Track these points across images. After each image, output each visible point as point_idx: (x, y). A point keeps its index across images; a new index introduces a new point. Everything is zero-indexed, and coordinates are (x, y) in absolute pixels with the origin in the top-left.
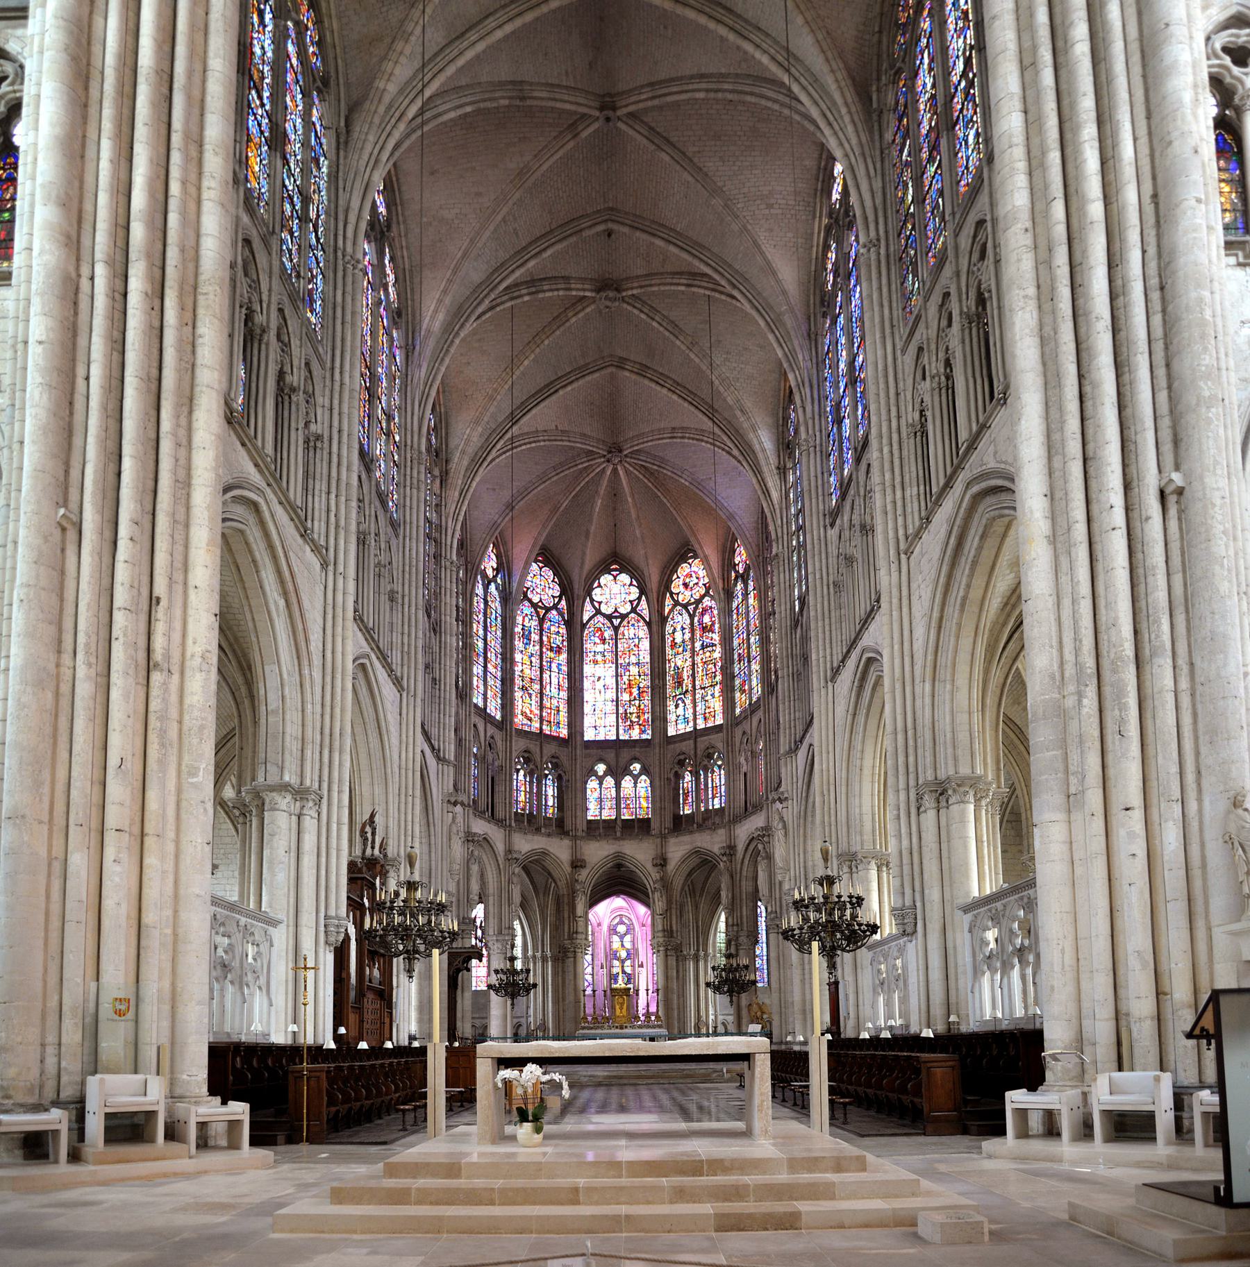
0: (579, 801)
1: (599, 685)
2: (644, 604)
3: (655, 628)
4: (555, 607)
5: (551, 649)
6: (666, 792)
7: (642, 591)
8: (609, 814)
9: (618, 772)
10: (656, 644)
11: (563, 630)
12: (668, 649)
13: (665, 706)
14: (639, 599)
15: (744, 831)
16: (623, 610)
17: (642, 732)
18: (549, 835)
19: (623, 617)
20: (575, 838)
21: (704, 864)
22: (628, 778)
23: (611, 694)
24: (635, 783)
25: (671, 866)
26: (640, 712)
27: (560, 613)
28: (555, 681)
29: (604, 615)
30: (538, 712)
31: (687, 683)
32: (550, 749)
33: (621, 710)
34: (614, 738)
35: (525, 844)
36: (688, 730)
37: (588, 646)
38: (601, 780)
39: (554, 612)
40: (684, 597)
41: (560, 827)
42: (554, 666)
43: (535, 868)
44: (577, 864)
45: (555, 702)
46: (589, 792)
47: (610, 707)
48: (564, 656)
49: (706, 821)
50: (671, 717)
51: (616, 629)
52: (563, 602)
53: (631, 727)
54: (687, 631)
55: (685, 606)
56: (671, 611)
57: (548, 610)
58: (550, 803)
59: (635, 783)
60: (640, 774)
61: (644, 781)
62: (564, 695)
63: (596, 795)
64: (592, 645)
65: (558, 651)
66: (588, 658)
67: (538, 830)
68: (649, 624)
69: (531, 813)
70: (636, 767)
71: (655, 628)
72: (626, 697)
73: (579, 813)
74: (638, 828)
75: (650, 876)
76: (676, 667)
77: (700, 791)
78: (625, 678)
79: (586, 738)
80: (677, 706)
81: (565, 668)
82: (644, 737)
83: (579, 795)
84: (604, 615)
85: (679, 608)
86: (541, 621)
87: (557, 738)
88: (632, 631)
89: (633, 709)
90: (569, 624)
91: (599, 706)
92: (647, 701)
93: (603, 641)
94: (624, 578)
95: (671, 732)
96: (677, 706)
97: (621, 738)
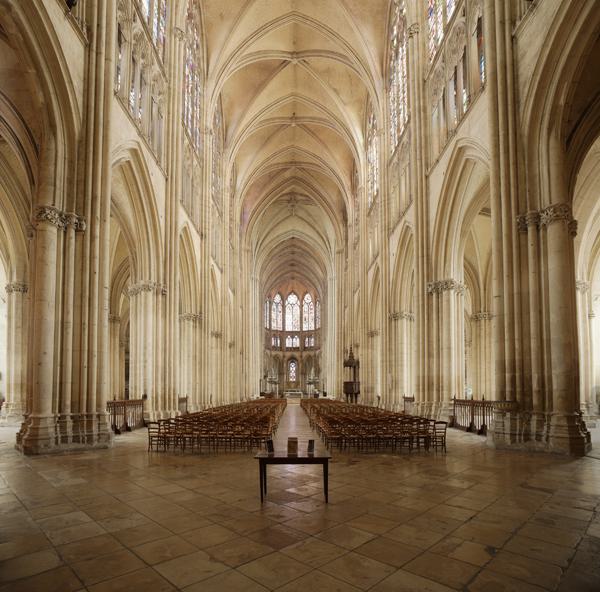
6: (302, 341)
9: (293, 337)
15: (317, 352)
21: (309, 358)
35: (274, 353)
41: (281, 349)
43: (276, 358)
44: (284, 356)
49: (310, 348)
64: (287, 310)
74: (296, 349)
75: (299, 359)
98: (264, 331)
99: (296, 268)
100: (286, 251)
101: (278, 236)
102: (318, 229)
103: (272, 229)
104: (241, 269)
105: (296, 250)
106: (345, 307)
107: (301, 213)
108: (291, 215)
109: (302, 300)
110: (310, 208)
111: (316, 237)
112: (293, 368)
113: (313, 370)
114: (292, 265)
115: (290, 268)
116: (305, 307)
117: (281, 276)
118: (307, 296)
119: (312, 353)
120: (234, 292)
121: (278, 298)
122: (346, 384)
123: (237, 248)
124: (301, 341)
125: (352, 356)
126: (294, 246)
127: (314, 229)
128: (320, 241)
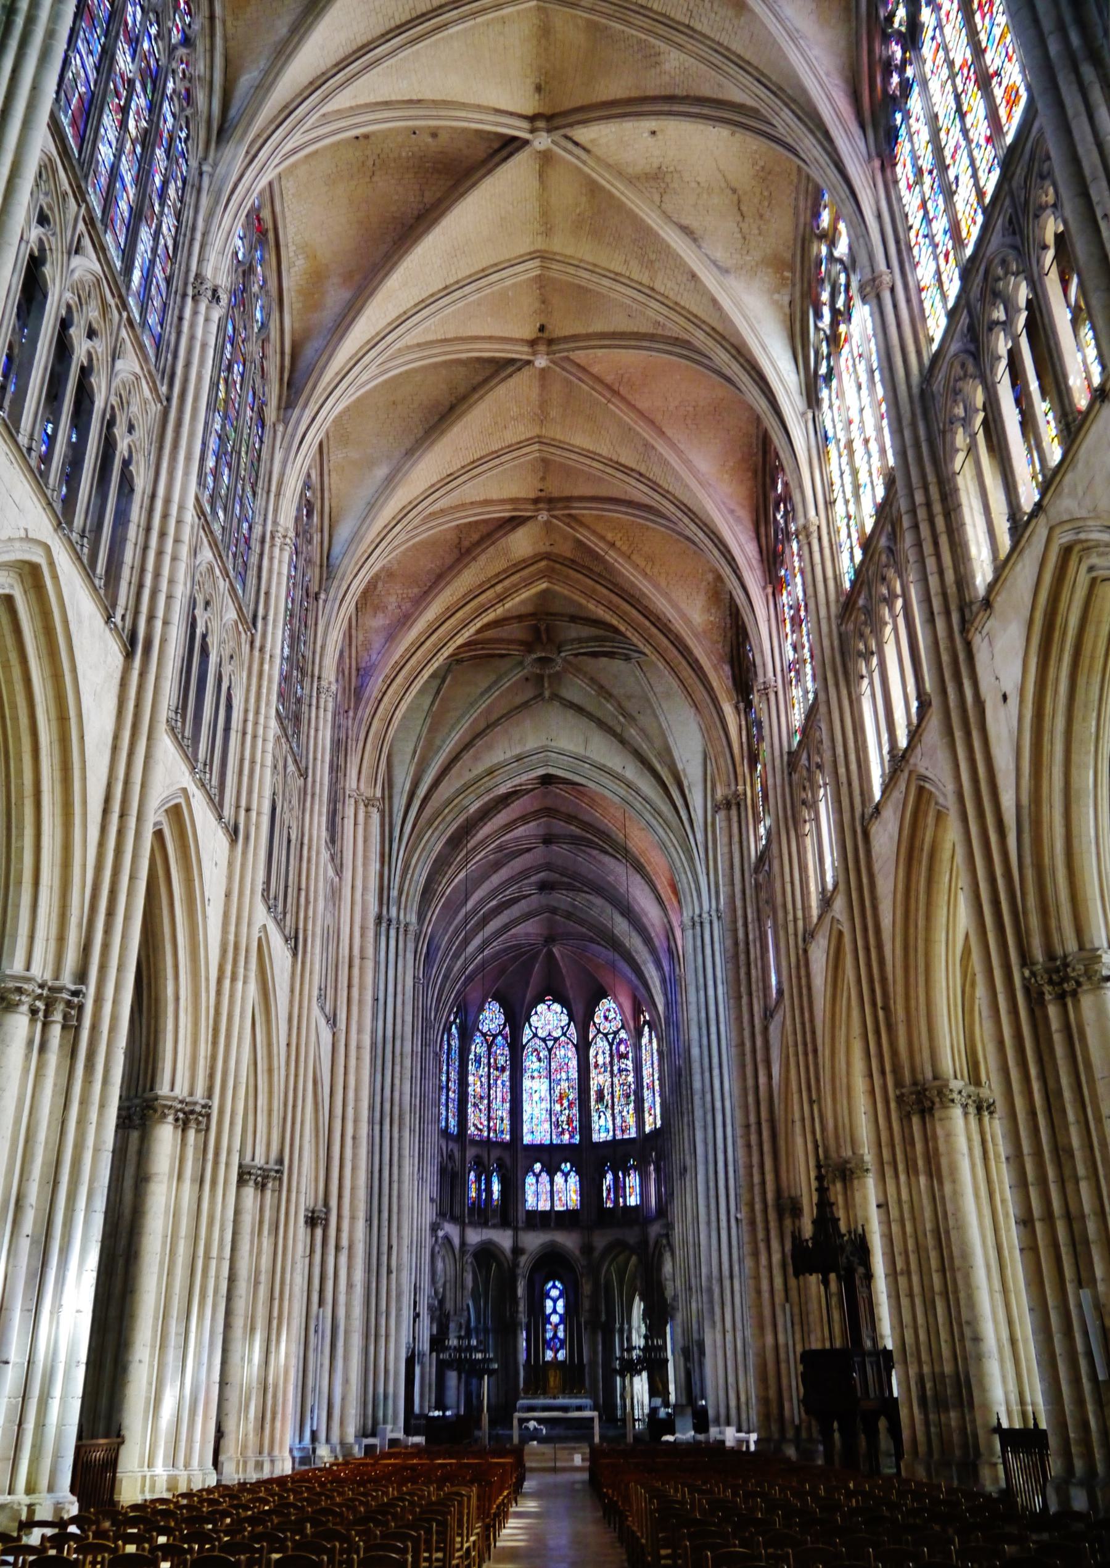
0: (520, 1197)
1: (536, 1097)
2: (572, 1028)
3: (581, 1053)
4: (500, 1033)
5: (497, 1069)
6: (590, 1189)
7: (571, 1017)
8: (544, 1205)
10: (582, 1063)
11: (506, 1052)
12: (592, 1067)
13: (589, 1116)
14: (569, 1024)
16: (555, 1034)
17: (571, 1137)
18: (494, 1226)
19: (556, 1039)
20: (516, 1229)
22: (559, 1174)
23: (546, 1105)
24: (566, 1181)
25: (596, 1254)
26: (570, 1121)
27: (505, 1038)
28: (499, 1095)
29: (540, 1038)
30: (486, 1123)
31: (608, 1097)
32: (495, 1153)
33: (554, 1119)
34: (548, 1142)
35: (475, 1237)
36: (609, 1138)
37: (526, 1064)
38: (537, 1176)
39: (500, 1038)
40: (606, 1027)
42: (499, 1082)
44: (517, 1251)
45: (499, 1113)
46: (527, 1186)
47: (545, 1116)
48: (507, 1073)
50: (595, 1126)
51: (550, 1050)
52: (507, 1029)
53: (562, 1133)
54: (607, 1055)
55: (606, 1035)
56: (595, 1037)
57: (495, 1036)
58: (496, 1196)
59: (566, 1181)
60: (569, 1172)
61: (573, 1179)
62: (507, 1105)
63: (533, 1188)
64: (531, 1063)
65: (503, 1069)
66: (526, 1075)
67: (484, 1224)
68: (576, 1046)
69: (479, 1206)
70: (566, 1167)
71: (581, 1053)
72: (558, 1107)
73: (520, 1208)
76: (598, 1084)
77: (619, 1188)
78: (557, 1092)
79: (525, 1142)
80: (600, 1117)
81: (508, 1084)
82: (573, 1141)
83: (520, 1192)
84: (540, 1038)
85: (601, 1035)
86: (489, 1047)
87: (502, 1144)
88: (563, 1052)
89: (564, 1118)
90: (509, 1046)
91: (536, 1112)
92: (575, 1110)
93: (539, 1060)
94: (557, 1007)
95: (596, 1137)
96: (600, 1117)
97: (554, 1142)
98: (433, 1139)
99: (561, 899)
100: (520, 831)
101: (490, 772)
102: (645, 747)
103: (466, 746)
104: (339, 871)
105: (560, 827)
106: (768, 1014)
107: (576, 690)
108: (539, 696)
109: (582, 1018)
110: (612, 669)
111: (631, 772)
112: (555, 1306)
113: (638, 1307)
114: (544, 887)
115: (536, 900)
116: (599, 1052)
117: (506, 928)
118: (606, 1004)
119: (631, 1236)
120: (294, 941)
121: (492, 1018)
122: (808, 1357)
123: (322, 774)
124: (583, 1192)
125: (825, 1218)
126: (548, 812)
127: (622, 741)
128: (647, 786)
